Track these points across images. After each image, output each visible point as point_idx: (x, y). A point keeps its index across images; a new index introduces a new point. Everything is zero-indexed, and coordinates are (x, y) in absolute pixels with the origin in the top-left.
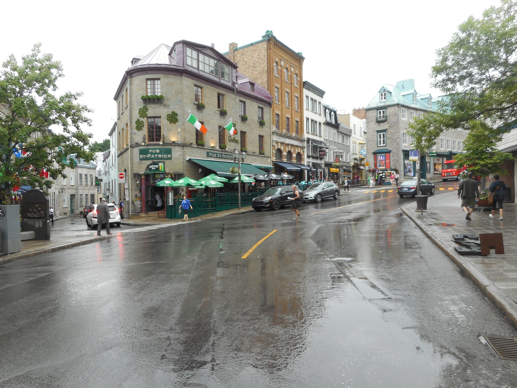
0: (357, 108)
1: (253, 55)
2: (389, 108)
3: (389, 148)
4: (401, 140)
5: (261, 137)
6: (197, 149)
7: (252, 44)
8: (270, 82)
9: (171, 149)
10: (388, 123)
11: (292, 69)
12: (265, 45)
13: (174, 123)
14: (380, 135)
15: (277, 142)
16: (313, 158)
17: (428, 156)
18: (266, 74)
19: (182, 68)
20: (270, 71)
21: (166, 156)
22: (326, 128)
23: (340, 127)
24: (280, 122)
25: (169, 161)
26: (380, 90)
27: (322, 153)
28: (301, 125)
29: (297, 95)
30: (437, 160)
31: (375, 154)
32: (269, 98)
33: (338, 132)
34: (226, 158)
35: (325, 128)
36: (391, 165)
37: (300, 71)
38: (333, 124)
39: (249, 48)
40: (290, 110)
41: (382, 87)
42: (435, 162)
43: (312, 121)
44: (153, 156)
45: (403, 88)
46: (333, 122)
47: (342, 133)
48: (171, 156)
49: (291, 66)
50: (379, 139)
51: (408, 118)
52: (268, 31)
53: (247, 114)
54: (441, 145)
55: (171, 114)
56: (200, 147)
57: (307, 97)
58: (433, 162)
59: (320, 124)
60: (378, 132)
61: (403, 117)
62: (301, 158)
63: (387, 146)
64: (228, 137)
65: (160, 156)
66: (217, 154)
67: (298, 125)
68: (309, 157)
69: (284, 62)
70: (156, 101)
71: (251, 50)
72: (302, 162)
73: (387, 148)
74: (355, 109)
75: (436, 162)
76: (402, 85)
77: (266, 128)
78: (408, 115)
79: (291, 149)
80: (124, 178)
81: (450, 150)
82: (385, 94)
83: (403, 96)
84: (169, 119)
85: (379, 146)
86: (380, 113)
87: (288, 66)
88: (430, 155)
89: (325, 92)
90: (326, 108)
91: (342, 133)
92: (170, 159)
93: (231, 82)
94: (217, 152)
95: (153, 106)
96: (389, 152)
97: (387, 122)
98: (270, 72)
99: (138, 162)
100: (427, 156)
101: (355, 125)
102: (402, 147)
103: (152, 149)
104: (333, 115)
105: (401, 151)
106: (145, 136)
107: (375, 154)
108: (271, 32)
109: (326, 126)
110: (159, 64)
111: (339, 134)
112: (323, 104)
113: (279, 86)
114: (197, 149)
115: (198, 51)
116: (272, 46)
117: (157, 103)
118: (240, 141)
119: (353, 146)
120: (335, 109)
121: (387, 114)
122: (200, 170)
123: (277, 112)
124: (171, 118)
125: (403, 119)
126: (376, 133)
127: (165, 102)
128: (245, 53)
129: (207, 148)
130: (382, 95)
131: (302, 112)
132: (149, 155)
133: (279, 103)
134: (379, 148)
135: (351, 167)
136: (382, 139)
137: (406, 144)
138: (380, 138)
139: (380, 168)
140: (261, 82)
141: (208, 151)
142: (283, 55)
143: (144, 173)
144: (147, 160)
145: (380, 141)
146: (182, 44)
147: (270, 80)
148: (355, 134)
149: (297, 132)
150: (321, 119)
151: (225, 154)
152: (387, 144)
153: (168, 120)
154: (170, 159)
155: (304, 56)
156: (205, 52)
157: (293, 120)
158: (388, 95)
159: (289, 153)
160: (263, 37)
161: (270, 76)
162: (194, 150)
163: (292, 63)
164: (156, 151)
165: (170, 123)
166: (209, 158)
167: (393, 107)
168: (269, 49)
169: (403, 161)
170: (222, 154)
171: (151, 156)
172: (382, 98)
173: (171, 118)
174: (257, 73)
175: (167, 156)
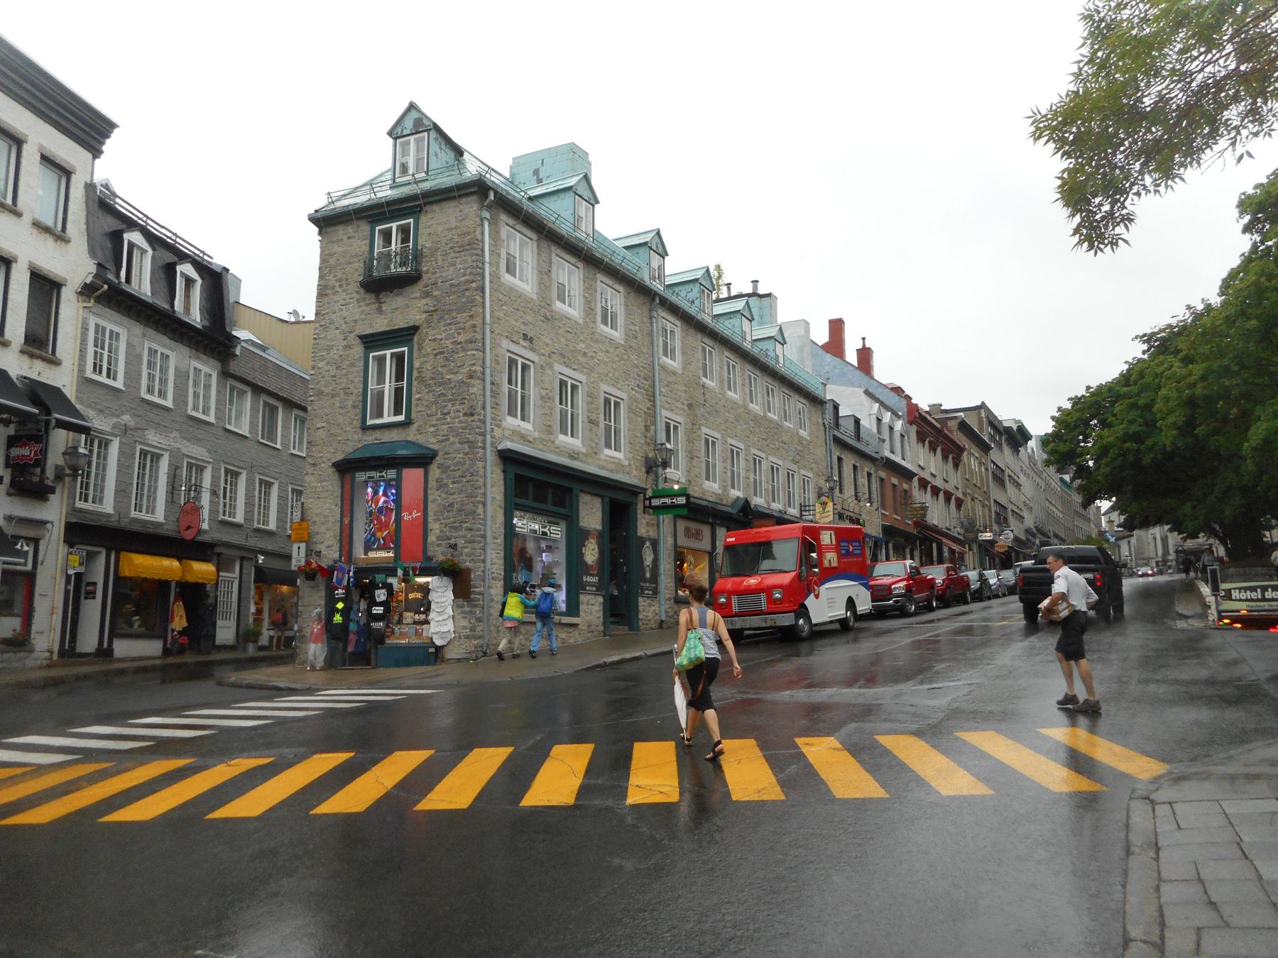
2: (436, 207)
3: (422, 436)
4: (495, 394)
10: (427, 295)
14: (381, 361)
17: (645, 507)
22: (110, 326)
23: (238, 351)
26: (399, 122)
27: (24, 451)
33: (225, 374)
35: (93, 321)
36: (432, 538)
41: (406, 106)
54: (704, 466)
58: (670, 541)
60: (372, 341)
61: (508, 271)
73: (411, 435)
75: (682, 541)
76: (536, 172)
81: (740, 494)
85: (369, 422)
86: (387, 235)
96: (423, 460)
97: (416, 290)
100: (640, 507)
102: (498, 432)
104: (189, 282)
105: (491, 457)
107: (346, 468)
111: (241, 394)
120: (219, 258)
121: (421, 242)
126: (358, 350)
134: (370, 438)
136: (388, 388)
137: (527, 426)
138: (381, 380)
139: (372, 555)
152: (413, 415)
167: (453, 204)
169: (501, 518)
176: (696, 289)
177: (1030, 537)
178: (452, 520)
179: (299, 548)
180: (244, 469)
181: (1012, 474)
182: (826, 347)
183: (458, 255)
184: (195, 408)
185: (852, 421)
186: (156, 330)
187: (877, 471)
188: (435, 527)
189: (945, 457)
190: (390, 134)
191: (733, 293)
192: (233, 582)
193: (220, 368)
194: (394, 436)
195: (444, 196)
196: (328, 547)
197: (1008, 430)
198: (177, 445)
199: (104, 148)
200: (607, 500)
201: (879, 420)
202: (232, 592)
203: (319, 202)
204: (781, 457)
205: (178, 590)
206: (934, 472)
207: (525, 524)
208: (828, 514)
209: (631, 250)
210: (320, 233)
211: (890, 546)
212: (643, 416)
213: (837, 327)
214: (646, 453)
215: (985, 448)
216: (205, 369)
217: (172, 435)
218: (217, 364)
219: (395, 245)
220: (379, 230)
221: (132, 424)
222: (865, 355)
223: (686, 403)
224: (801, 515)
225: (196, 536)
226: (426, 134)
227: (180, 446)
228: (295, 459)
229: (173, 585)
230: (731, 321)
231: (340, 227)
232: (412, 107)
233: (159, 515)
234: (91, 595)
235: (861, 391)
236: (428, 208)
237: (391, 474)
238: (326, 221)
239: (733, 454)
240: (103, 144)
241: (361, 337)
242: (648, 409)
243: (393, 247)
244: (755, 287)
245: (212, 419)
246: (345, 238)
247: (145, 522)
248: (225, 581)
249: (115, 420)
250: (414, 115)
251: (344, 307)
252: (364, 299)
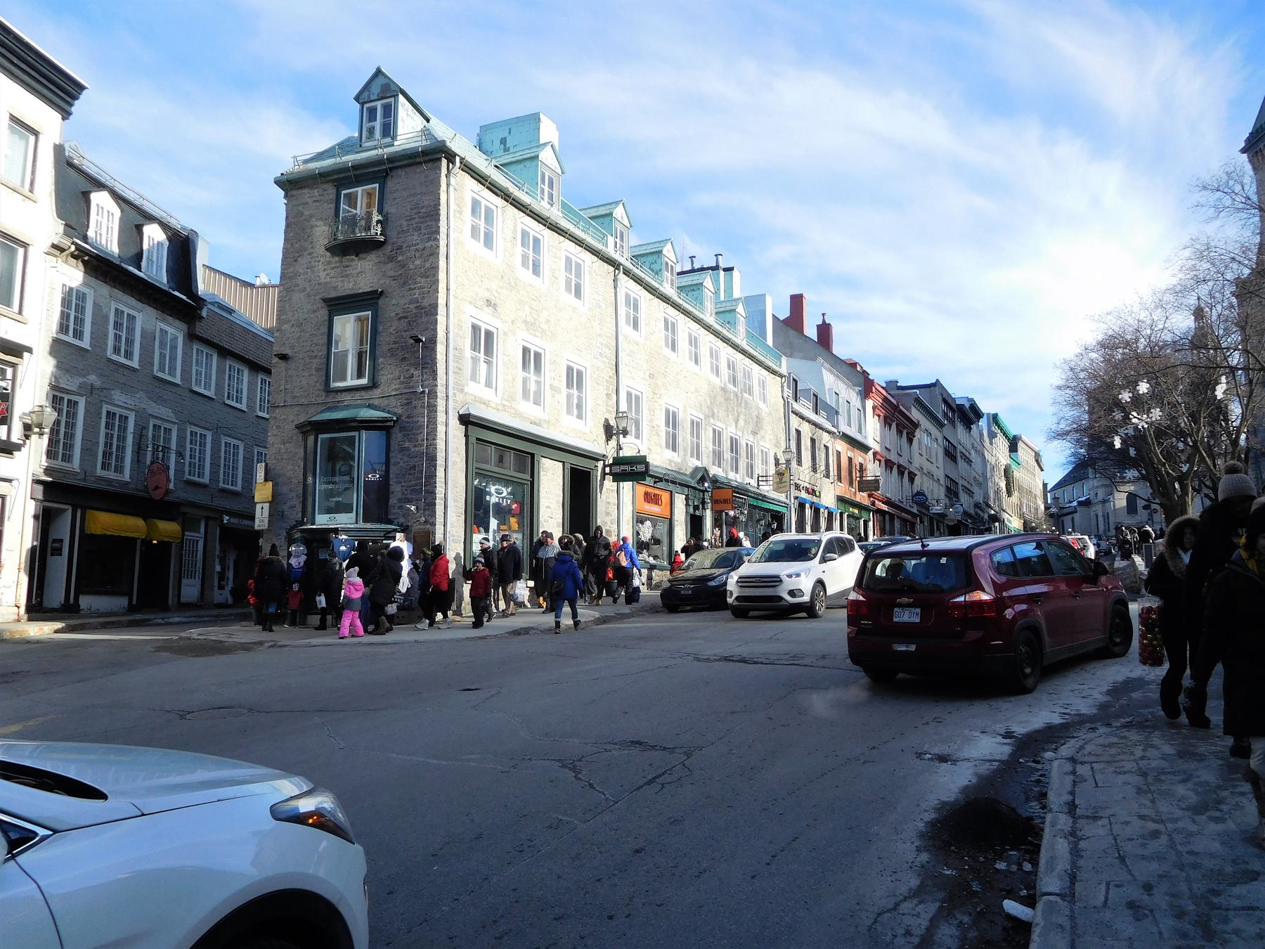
2: (399, 172)
23: (204, 313)
30: (649, 498)
33: (192, 337)
46: (156, 271)
63: (377, 393)
76: (503, 141)
86: (352, 201)
172: (371, 131)
177: (979, 512)
178: (413, 482)
179: (262, 508)
180: (210, 430)
181: (964, 451)
182: (786, 322)
183: (423, 220)
184: (162, 369)
186: (123, 291)
187: (833, 443)
189: (900, 432)
190: (357, 99)
191: (696, 266)
192: (197, 541)
193: (186, 330)
195: (411, 161)
196: (293, 507)
197: (961, 407)
198: (143, 405)
199: (73, 109)
200: (568, 466)
202: (197, 551)
203: (287, 166)
205: (143, 548)
206: (888, 447)
208: (786, 484)
209: (596, 220)
210: (286, 196)
211: (845, 516)
212: (605, 384)
213: (797, 301)
214: (607, 420)
215: (940, 425)
216: (170, 330)
217: (138, 396)
218: (184, 327)
220: (345, 194)
221: (98, 383)
222: (825, 330)
223: (647, 374)
224: (758, 485)
225: (164, 496)
226: (392, 99)
227: (146, 407)
228: (261, 421)
229: (139, 542)
230: (694, 293)
231: (305, 191)
232: (379, 72)
234: (57, 552)
236: (394, 173)
238: (289, 184)
240: (71, 105)
241: (325, 300)
242: (610, 377)
243: (358, 211)
245: (178, 380)
246: (310, 200)
247: (110, 481)
248: (190, 540)
249: (81, 380)
250: (380, 81)
251: (309, 270)
252: (329, 263)
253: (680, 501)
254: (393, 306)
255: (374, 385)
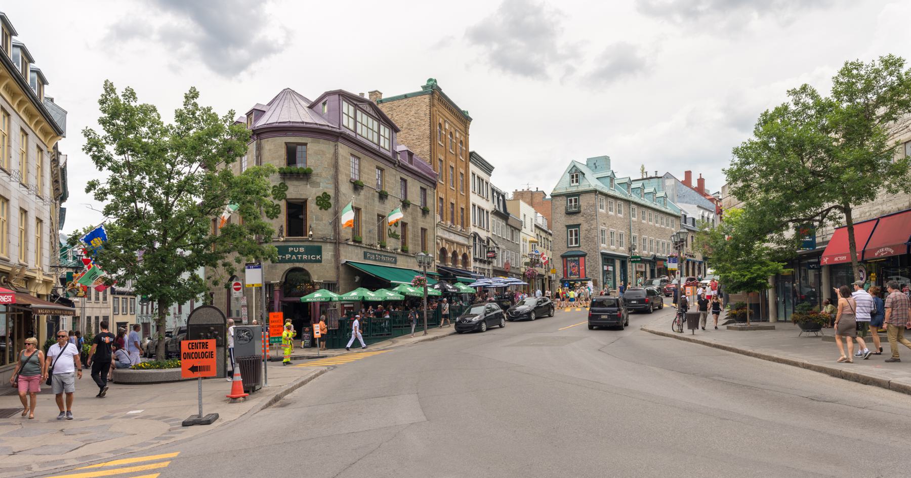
0: (520, 190)
1: (407, 112)
3: (584, 249)
5: (424, 230)
6: (353, 248)
7: (406, 96)
8: (434, 153)
9: (320, 247)
10: (583, 216)
11: (458, 135)
12: (427, 99)
13: (326, 210)
14: (571, 232)
15: (442, 239)
16: (481, 261)
18: (429, 141)
19: (338, 130)
20: (432, 138)
21: (313, 257)
24: (444, 209)
25: (318, 264)
26: (571, 170)
27: (491, 254)
28: (467, 214)
29: (463, 171)
31: (564, 257)
32: (432, 175)
34: (385, 262)
36: (587, 273)
37: (465, 137)
38: (501, 213)
39: (401, 101)
40: (455, 193)
42: (637, 270)
43: (479, 208)
44: (294, 257)
45: (596, 167)
47: (511, 226)
48: (321, 257)
49: (456, 130)
50: (569, 237)
51: (607, 209)
52: (430, 80)
53: (409, 198)
55: (321, 196)
56: (357, 244)
57: (474, 174)
59: (487, 212)
60: (568, 227)
62: (466, 261)
64: (387, 230)
65: (305, 257)
66: (375, 254)
67: (463, 214)
68: (475, 260)
69: (449, 124)
70: (301, 177)
71: (405, 105)
72: (467, 268)
74: (516, 190)
76: (595, 164)
77: (429, 218)
78: (607, 206)
79: (457, 249)
80: (241, 290)
82: (577, 176)
83: (597, 178)
84: (318, 203)
86: (571, 201)
87: (453, 130)
88: (632, 260)
89: (494, 168)
90: (493, 190)
91: (511, 226)
92: (320, 261)
93: (391, 151)
94: (376, 252)
95: (296, 183)
96: (584, 255)
98: (434, 138)
99: (269, 266)
101: (525, 215)
103: (293, 247)
106: (282, 226)
107: (564, 257)
108: (435, 81)
109: (494, 216)
110: (306, 123)
112: (490, 185)
113: (442, 158)
114: (354, 247)
115: (355, 106)
116: (436, 102)
117: (301, 179)
118: (400, 237)
119: (523, 245)
122: (357, 279)
123: (442, 195)
124: (322, 202)
125: (601, 210)
126: (565, 229)
127: (314, 178)
128: (394, 107)
129: (364, 245)
130: (573, 177)
131: (467, 197)
132: (288, 256)
133: (443, 183)
134: (569, 250)
135: (521, 275)
136: (574, 237)
138: (571, 235)
139: (572, 277)
140: (422, 150)
141: (366, 250)
142: (447, 113)
143: (278, 281)
144: (284, 263)
145: (571, 240)
146: (337, 96)
147: (434, 149)
148: (525, 228)
149: (462, 225)
150: (489, 206)
151: (385, 256)
153: (317, 205)
154: (320, 261)
155: (470, 115)
156: (363, 108)
157: (459, 206)
158: (581, 176)
159: (455, 254)
160: (423, 87)
161: (434, 144)
162: (350, 248)
163: (457, 126)
164: (299, 249)
165: (321, 209)
166: (367, 261)
168: (432, 105)
170: (381, 255)
171: (292, 257)
172: (573, 181)
173: (322, 202)
174: (414, 138)
175: (316, 257)
176: (639, 190)
182: (682, 182)
185: (692, 219)
188: (588, 270)
194: (576, 249)
201: (703, 217)
204: (666, 239)
207: (605, 268)
219: (573, 204)
233: (500, 266)
235: (696, 206)
237: (577, 258)
239: (651, 241)
244: (656, 174)
253: (648, 265)
254: (584, 227)
255: (579, 247)
